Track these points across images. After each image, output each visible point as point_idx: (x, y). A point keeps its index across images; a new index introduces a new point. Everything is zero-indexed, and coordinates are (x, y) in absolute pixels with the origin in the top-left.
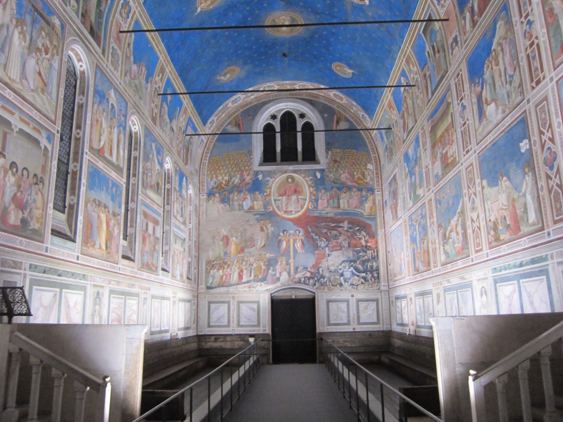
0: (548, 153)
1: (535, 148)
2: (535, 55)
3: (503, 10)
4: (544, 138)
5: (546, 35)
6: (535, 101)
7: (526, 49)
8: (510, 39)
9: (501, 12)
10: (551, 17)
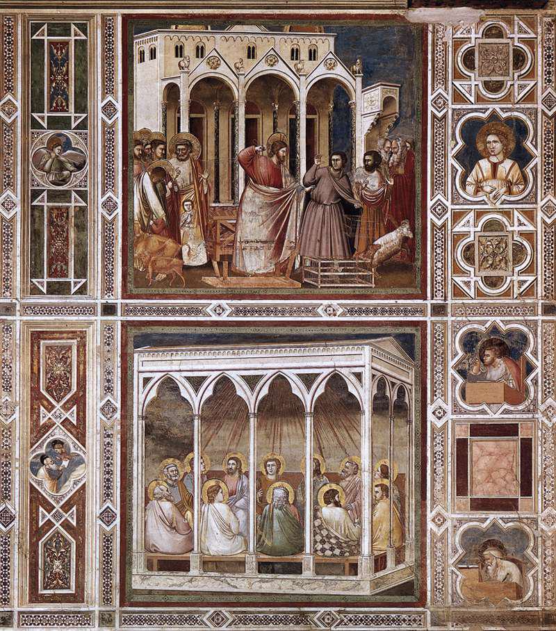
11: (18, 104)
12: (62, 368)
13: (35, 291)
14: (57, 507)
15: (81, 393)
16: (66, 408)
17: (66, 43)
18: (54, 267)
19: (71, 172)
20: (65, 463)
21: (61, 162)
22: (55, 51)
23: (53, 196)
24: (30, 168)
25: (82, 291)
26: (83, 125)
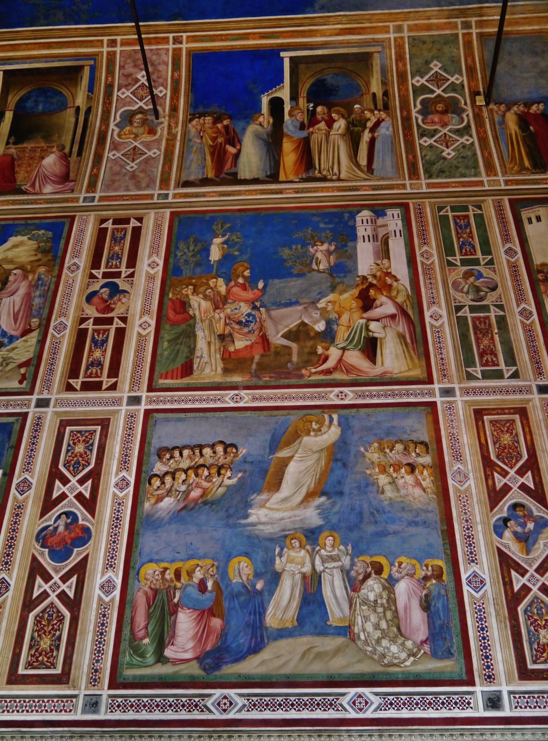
0: (61, 523)
1: (20, 498)
2: (105, 341)
3: (47, 229)
4: (59, 488)
5: (152, 329)
6: (66, 412)
7: (83, 320)
8: (39, 279)
9: (47, 227)
10: (176, 313)
11: (434, 252)
12: (510, 439)
13: (470, 377)
14: (531, 571)
15: (533, 460)
16: (521, 472)
17: (467, 217)
18: (485, 359)
19: (487, 292)
20: (531, 526)
21: (476, 287)
22: (458, 221)
23: (473, 309)
24: (451, 292)
25: (515, 375)
26: (491, 262)
